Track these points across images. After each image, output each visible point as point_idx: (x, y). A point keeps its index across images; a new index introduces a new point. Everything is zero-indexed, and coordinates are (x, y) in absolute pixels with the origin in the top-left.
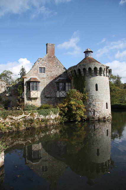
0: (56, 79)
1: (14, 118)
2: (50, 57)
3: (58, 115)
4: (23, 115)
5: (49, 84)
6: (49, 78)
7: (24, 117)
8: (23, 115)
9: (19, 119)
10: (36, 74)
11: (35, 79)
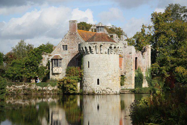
0: (76, 55)
1: (16, 86)
2: (72, 34)
3: (56, 88)
4: (23, 85)
5: (71, 61)
6: (71, 54)
7: (24, 87)
8: (23, 85)
9: (20, 88)
10: (60, 52)
11: (57, 56)
